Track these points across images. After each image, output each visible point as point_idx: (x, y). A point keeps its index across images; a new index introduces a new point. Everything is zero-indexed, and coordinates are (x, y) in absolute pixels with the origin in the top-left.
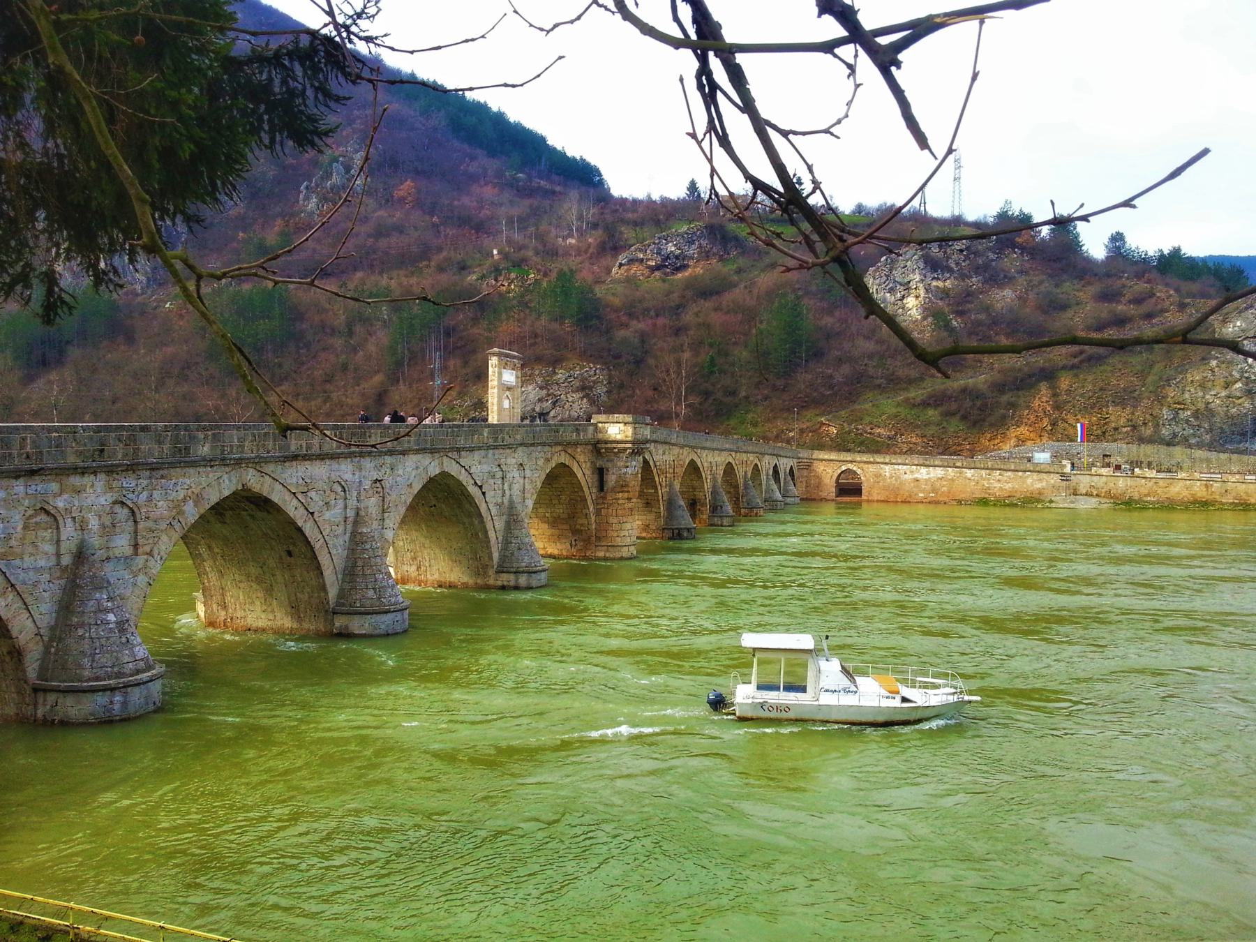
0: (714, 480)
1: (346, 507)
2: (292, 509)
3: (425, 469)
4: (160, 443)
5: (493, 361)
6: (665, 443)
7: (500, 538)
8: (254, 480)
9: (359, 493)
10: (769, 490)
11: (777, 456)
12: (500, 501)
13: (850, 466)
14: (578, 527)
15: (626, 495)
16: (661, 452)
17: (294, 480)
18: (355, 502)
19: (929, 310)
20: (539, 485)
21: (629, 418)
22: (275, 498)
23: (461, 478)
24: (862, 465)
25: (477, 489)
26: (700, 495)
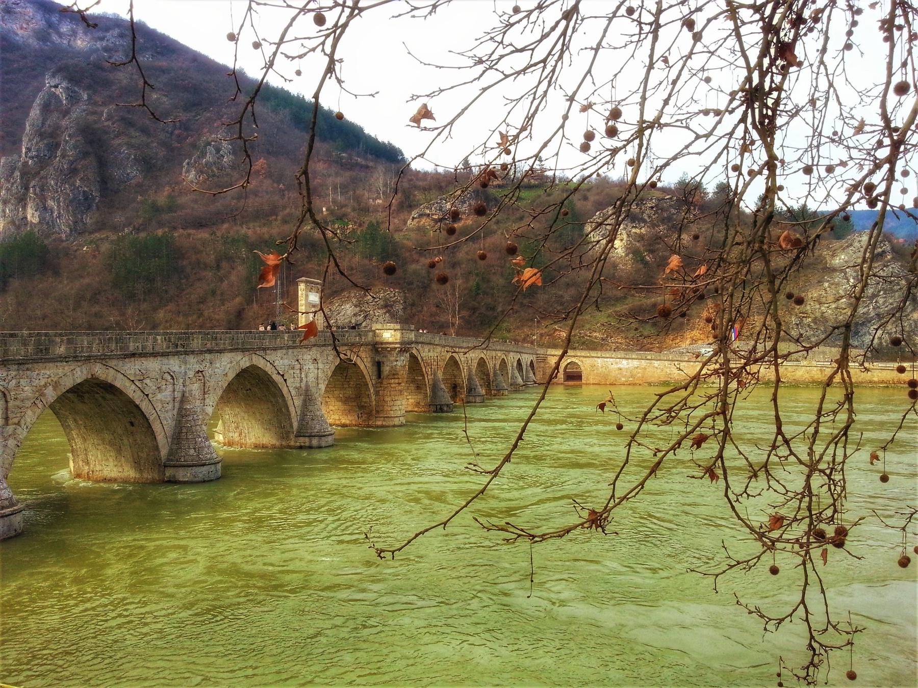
0: (470, 370)
1: (174, 391)
2: (131, 391)
3: (238, 363)
4: (25, 345)
5: (302, 286)
6: (430, 344)
7: (299, 413)
8: (100, 371)
9: (185, 381)
10: (513, 377)
11: (520, 353)
12: (298, 385)
13: (574, 360)
14: (363, 404)
15: (397, 381)
16: (427, 350)
17: (132, 372)
18: (182, 387)
19: (631, 250)
20: (330, 374)
21: (398, 326)
22: (118, 384)
23: (267, 369)
24: (581, 358)
25: (280, 377)
26: (459, 381)
